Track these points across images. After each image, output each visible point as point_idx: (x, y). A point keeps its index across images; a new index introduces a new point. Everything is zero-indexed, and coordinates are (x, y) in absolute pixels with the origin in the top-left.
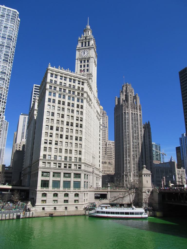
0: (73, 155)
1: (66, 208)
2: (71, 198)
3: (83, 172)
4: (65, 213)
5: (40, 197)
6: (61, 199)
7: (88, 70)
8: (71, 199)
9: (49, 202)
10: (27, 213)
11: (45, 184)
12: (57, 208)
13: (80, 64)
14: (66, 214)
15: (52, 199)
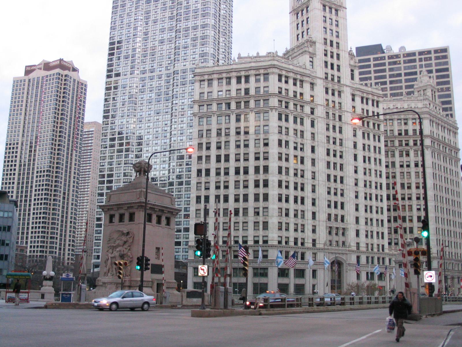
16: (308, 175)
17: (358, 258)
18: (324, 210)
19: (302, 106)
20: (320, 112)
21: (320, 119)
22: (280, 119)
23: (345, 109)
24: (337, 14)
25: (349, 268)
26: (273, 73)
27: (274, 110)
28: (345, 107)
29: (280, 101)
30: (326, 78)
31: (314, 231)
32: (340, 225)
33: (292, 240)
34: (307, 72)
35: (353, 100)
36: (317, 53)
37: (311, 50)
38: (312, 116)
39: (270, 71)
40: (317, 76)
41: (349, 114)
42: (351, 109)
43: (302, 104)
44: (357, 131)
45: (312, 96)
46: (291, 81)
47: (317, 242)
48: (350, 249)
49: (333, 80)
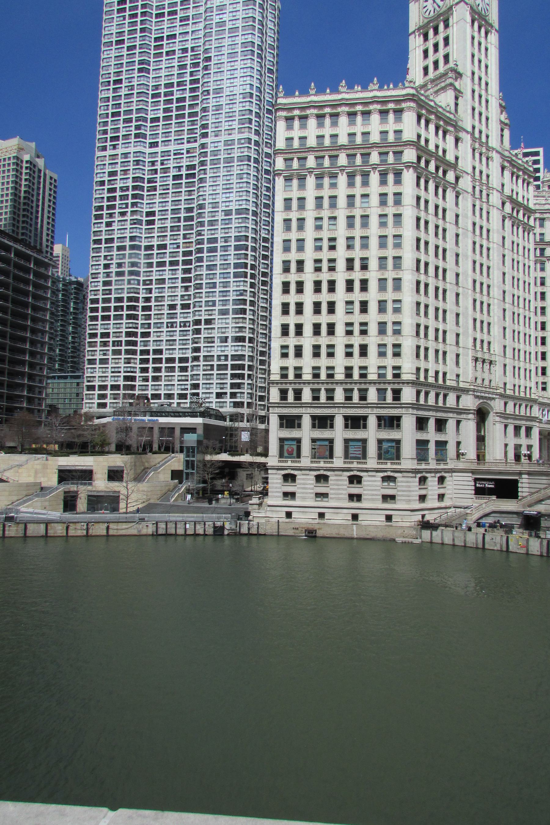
0: (372, 361)
1: (355, 517)
2: (369, 488)
3: (338, 411)
4: (353, 530)
5: (277, 483)
6: (340, 492)
7: (446, 57)
8: (370, 492)
9: (304, 498)
10: (242, 522)
11: (291, 449)
12: (327, 516)
13: (422, 48)
14: (355, 533)
15: (312, 491)
17: (506, 404)
19: (445, 173)
20: (466, 183)
21: (465, 194)
22: (418, 185)
23: (495, 186)
25: (498, 419)
26: (409, 108)
27: (411, 170)
29: (419, 158)
33: (431, 373)
34: (452, 116)
37: (457, 84)
39: (404, 105)
41: (499, 194)
42: (499, 189)
43: (446, 168)
44: (507, 221)
45: (457, 158)
46: (432, 127)
47: (461, 379)
48: (498, 391)
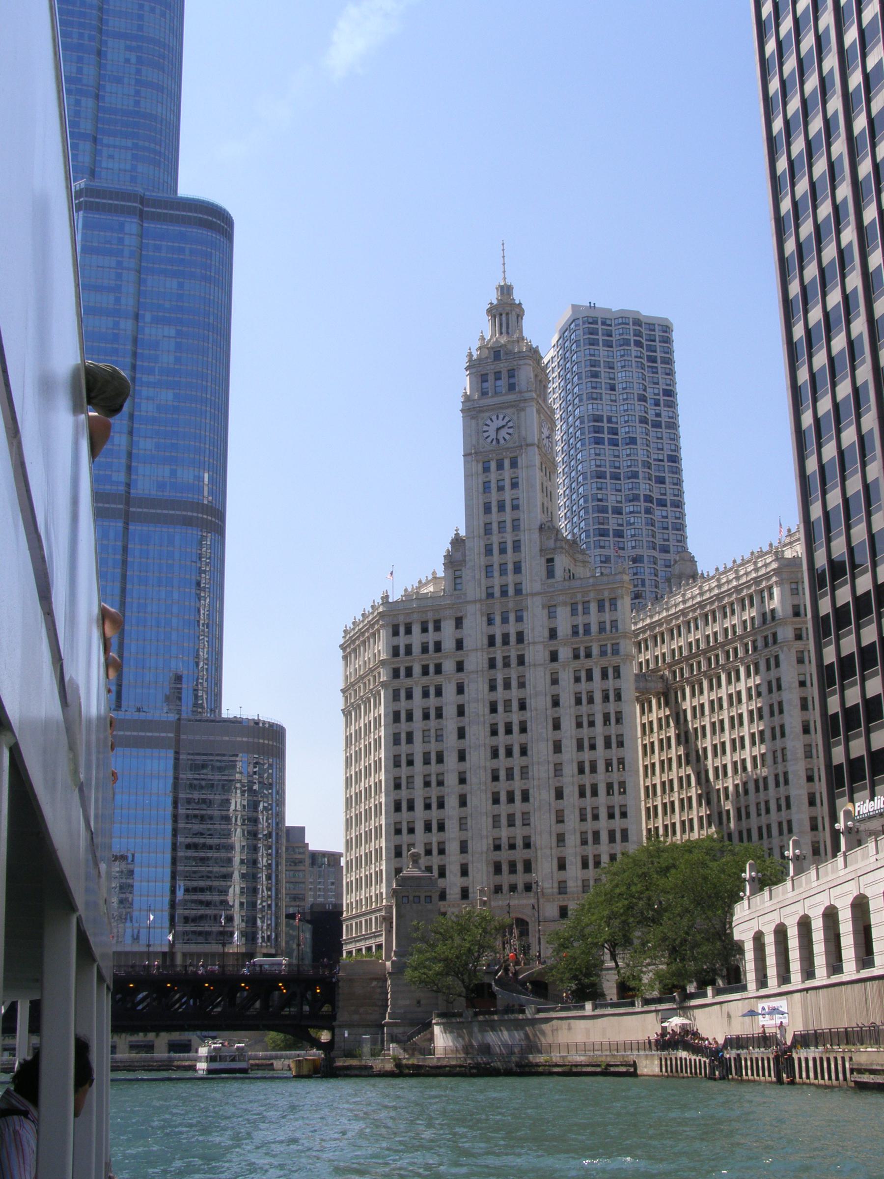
16: (451, 780)
18: (484, 833)
20: (476, 660)
24: (514, 464)
28: (528, 637)
30: (490, 595)
31: (464, 872)
32: (519, 855)
35: (552, 615)
36: (467, 558)
38: (460, 675)
40: (468, 599)
41: (540, 647)
46: (416, 629)
49: (504, 593)
